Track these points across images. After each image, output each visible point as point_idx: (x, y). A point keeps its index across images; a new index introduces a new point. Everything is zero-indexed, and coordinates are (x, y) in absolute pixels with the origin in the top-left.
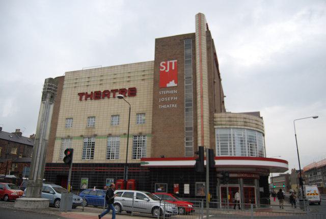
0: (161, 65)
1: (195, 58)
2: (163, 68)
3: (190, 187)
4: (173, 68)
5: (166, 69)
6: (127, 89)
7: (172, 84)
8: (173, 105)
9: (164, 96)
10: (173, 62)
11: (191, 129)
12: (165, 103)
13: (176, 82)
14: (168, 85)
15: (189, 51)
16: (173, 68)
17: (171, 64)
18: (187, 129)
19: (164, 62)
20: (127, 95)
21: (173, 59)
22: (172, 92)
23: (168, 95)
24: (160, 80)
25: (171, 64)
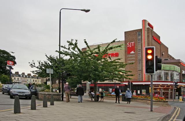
0: (128, 44)
1: (142, 41)
2: (128, 45)
3: (140, 91)
4: (133, 46)
5: (130, 46)
6: (114, 53)
7: (132, 52)
8: (133, 61)
9: (129, 57)
10: (133, 42)
11: (140, 70)
12: (129, 60)
13: (134, 52)
14: (131, 53)
15: (140, 37)
16: (133, 46)
17: (132, 43)
18: (139, 70)
19: (129, 43)
20: (115, 56)
21: (133, 42)
22: (132, 56)
23: (131, 57)
24: (129, 50)
25: (132, 43)
